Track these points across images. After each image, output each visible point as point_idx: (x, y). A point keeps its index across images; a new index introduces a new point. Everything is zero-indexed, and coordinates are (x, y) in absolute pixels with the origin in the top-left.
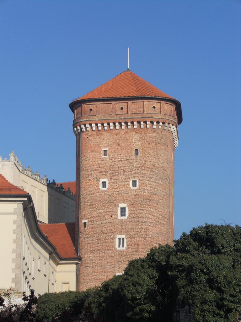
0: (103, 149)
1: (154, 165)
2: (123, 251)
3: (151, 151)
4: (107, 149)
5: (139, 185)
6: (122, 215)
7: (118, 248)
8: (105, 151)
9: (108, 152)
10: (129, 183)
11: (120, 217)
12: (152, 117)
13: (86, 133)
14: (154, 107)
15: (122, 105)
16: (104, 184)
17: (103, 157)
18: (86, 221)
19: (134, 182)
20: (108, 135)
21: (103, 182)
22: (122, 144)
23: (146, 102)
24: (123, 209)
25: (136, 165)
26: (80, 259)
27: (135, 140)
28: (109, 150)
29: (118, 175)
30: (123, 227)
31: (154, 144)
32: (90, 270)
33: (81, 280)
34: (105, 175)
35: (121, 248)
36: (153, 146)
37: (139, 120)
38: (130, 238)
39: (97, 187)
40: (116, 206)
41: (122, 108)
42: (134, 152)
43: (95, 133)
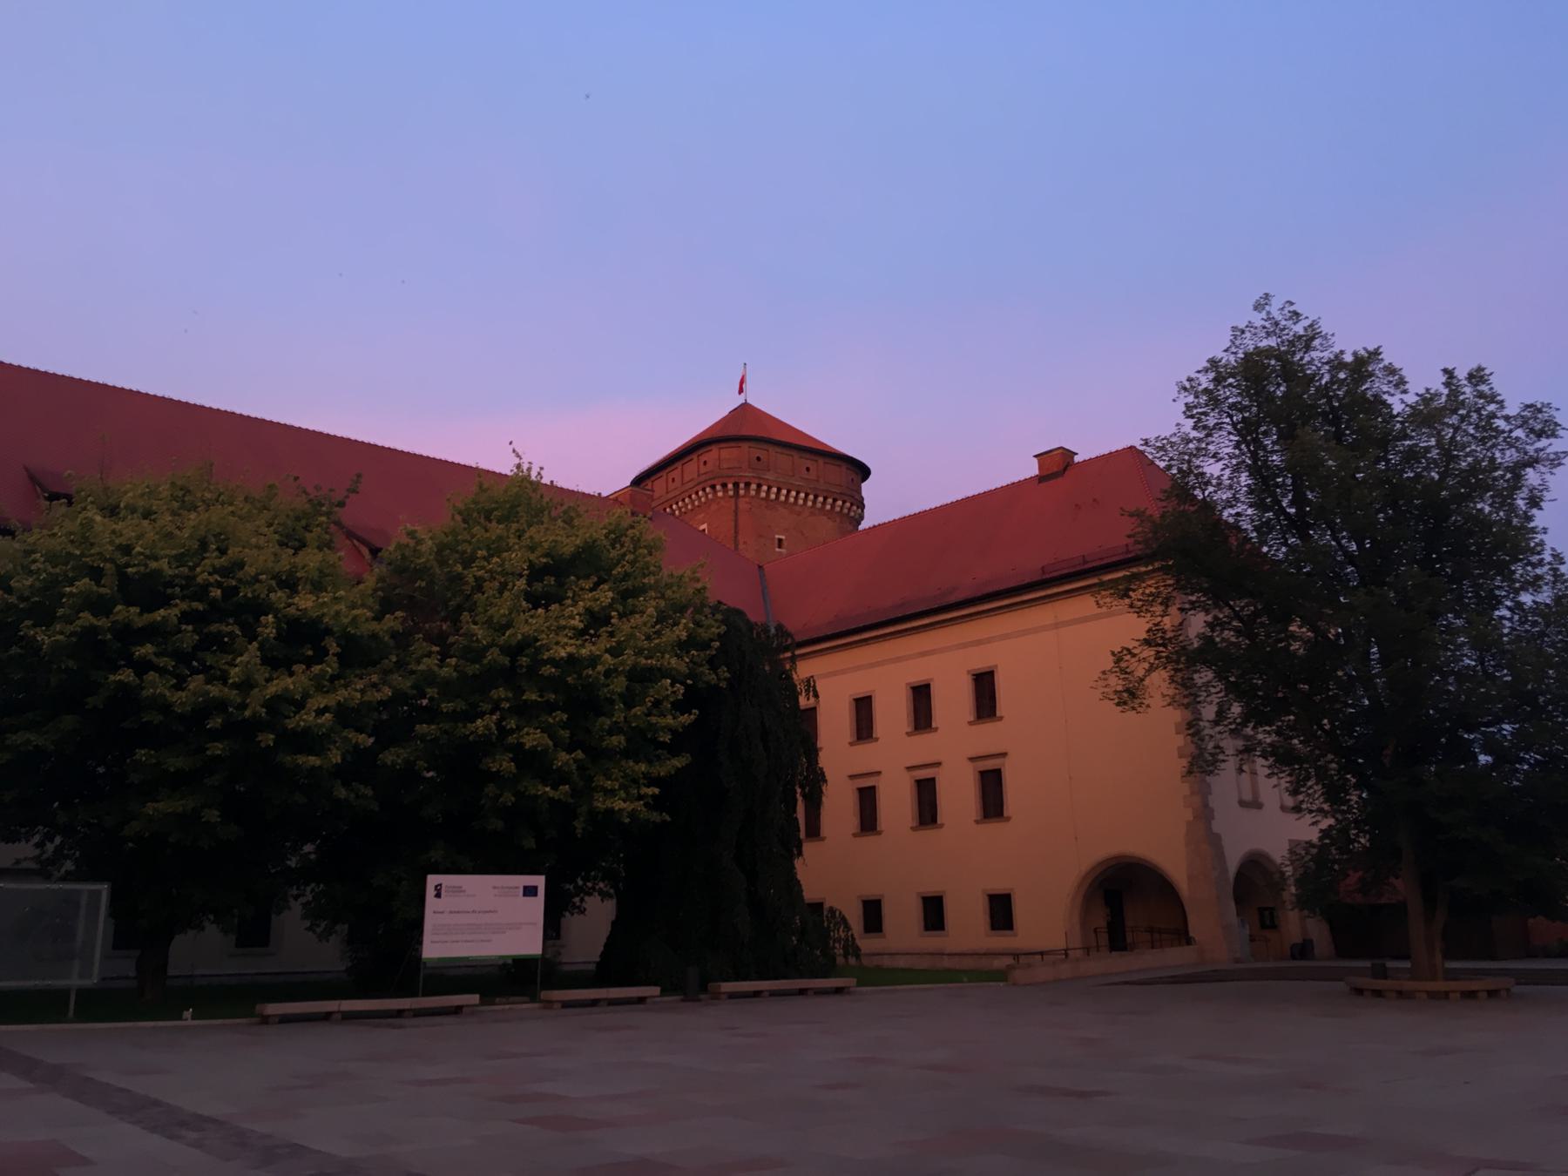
0: (777, 536)
4: (783, 537)
8: (780, 540)
9: (785, 544)
13: (747, 499)
15: (809, 464)
17: (777, 550)
28: (786, 539)
37: (836, 496)
41: (808, 469)
43: (763, 502)
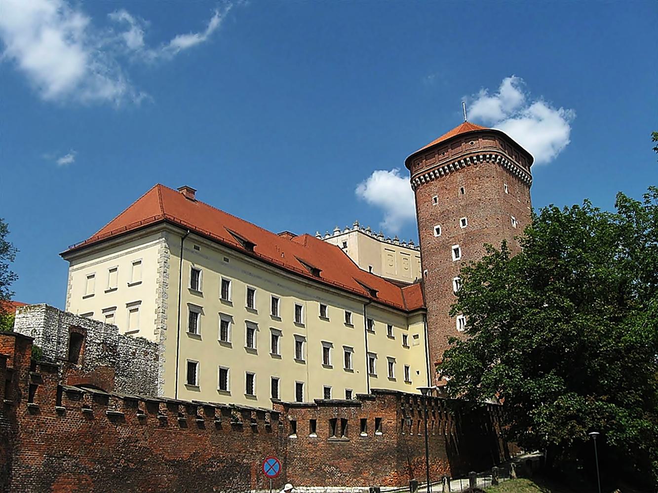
1: (480, 200)
3: (475, 187)
5: (468, 222)
6: (456, 257)
10: (459, 223)
11: (454, 259)
12: (471, 153)
16: (438, 230)
19: (463, 221)
21: (436, 229)
22: (448, 188)
24: (456, 251)
26: (426, 310)
31: (477, 179)
32: (434, 318)
36: (476, 181)
40: (450, 250)
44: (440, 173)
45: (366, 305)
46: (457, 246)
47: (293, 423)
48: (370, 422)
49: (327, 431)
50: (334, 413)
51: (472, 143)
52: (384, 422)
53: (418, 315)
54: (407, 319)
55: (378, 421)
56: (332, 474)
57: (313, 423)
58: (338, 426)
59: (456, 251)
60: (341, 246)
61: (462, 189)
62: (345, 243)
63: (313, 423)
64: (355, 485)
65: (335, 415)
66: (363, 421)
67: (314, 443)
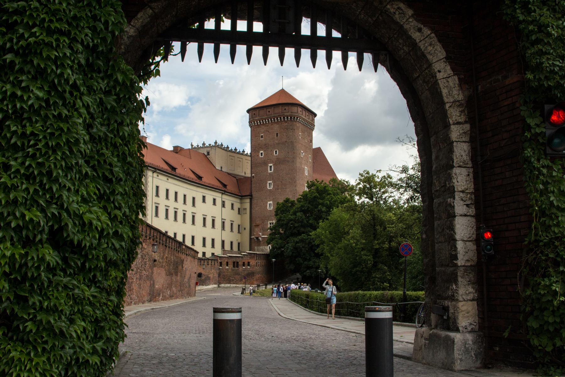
1: (286, 141)
2: (271, 190)
7: (269, 188)
8: (262, 136)
14: (285, 109)
16: (262, 153)
18: (253, 175)
19: (276, 151)
20: (263, 127)
22: (270, 131)
23: (280, 107)
24: (271, 167)
25: (277, 142)
27: (276, 127)
29: (268, 148)
30: (271, 177)
31: (286, 130)
33: (252, 207)
34: (262, 149)
35: (270, 188)
38: (274, 182)
39: (258, 156)
42: (276, 135)
44: (266, 122)
45: (222, 194)
46: (271, 165)
47: (221, 263)
48: (246, 263)
49: (232, 266)
50: (234, 260)
51: (285, 109)
52: (251, 263)
53: (247, 198)
54: (241, 199)
55: (249, 263)
56: (233, 280)
57: (227, 263)
58: (236, 264)
59: (271, 167)
60: (206, 154)
61: (277, 134)
62: (208, 153)
63: (227, 263)
64: (241, 284)
65: (235, 260)
66: (244, 263)
67: (227, 270)
